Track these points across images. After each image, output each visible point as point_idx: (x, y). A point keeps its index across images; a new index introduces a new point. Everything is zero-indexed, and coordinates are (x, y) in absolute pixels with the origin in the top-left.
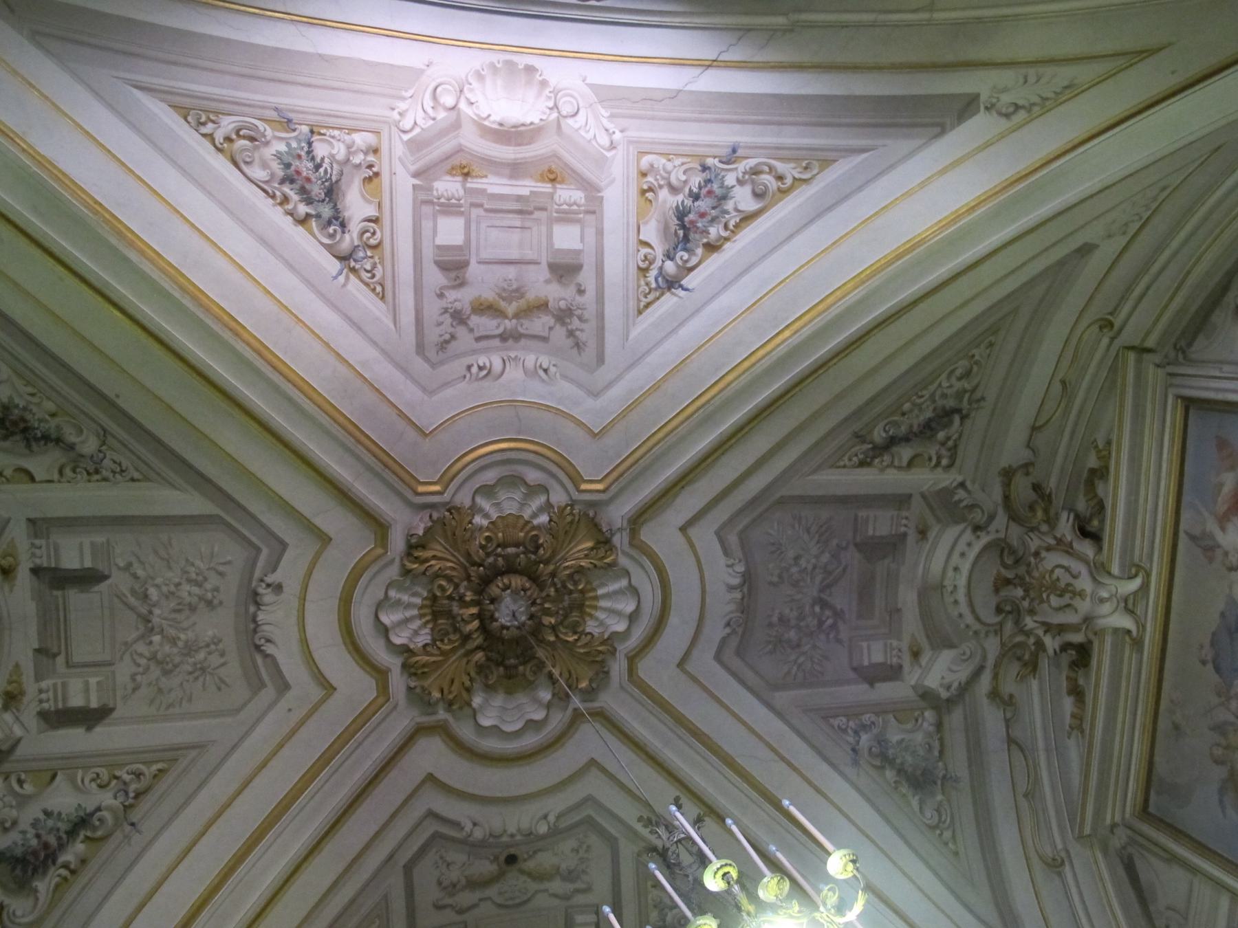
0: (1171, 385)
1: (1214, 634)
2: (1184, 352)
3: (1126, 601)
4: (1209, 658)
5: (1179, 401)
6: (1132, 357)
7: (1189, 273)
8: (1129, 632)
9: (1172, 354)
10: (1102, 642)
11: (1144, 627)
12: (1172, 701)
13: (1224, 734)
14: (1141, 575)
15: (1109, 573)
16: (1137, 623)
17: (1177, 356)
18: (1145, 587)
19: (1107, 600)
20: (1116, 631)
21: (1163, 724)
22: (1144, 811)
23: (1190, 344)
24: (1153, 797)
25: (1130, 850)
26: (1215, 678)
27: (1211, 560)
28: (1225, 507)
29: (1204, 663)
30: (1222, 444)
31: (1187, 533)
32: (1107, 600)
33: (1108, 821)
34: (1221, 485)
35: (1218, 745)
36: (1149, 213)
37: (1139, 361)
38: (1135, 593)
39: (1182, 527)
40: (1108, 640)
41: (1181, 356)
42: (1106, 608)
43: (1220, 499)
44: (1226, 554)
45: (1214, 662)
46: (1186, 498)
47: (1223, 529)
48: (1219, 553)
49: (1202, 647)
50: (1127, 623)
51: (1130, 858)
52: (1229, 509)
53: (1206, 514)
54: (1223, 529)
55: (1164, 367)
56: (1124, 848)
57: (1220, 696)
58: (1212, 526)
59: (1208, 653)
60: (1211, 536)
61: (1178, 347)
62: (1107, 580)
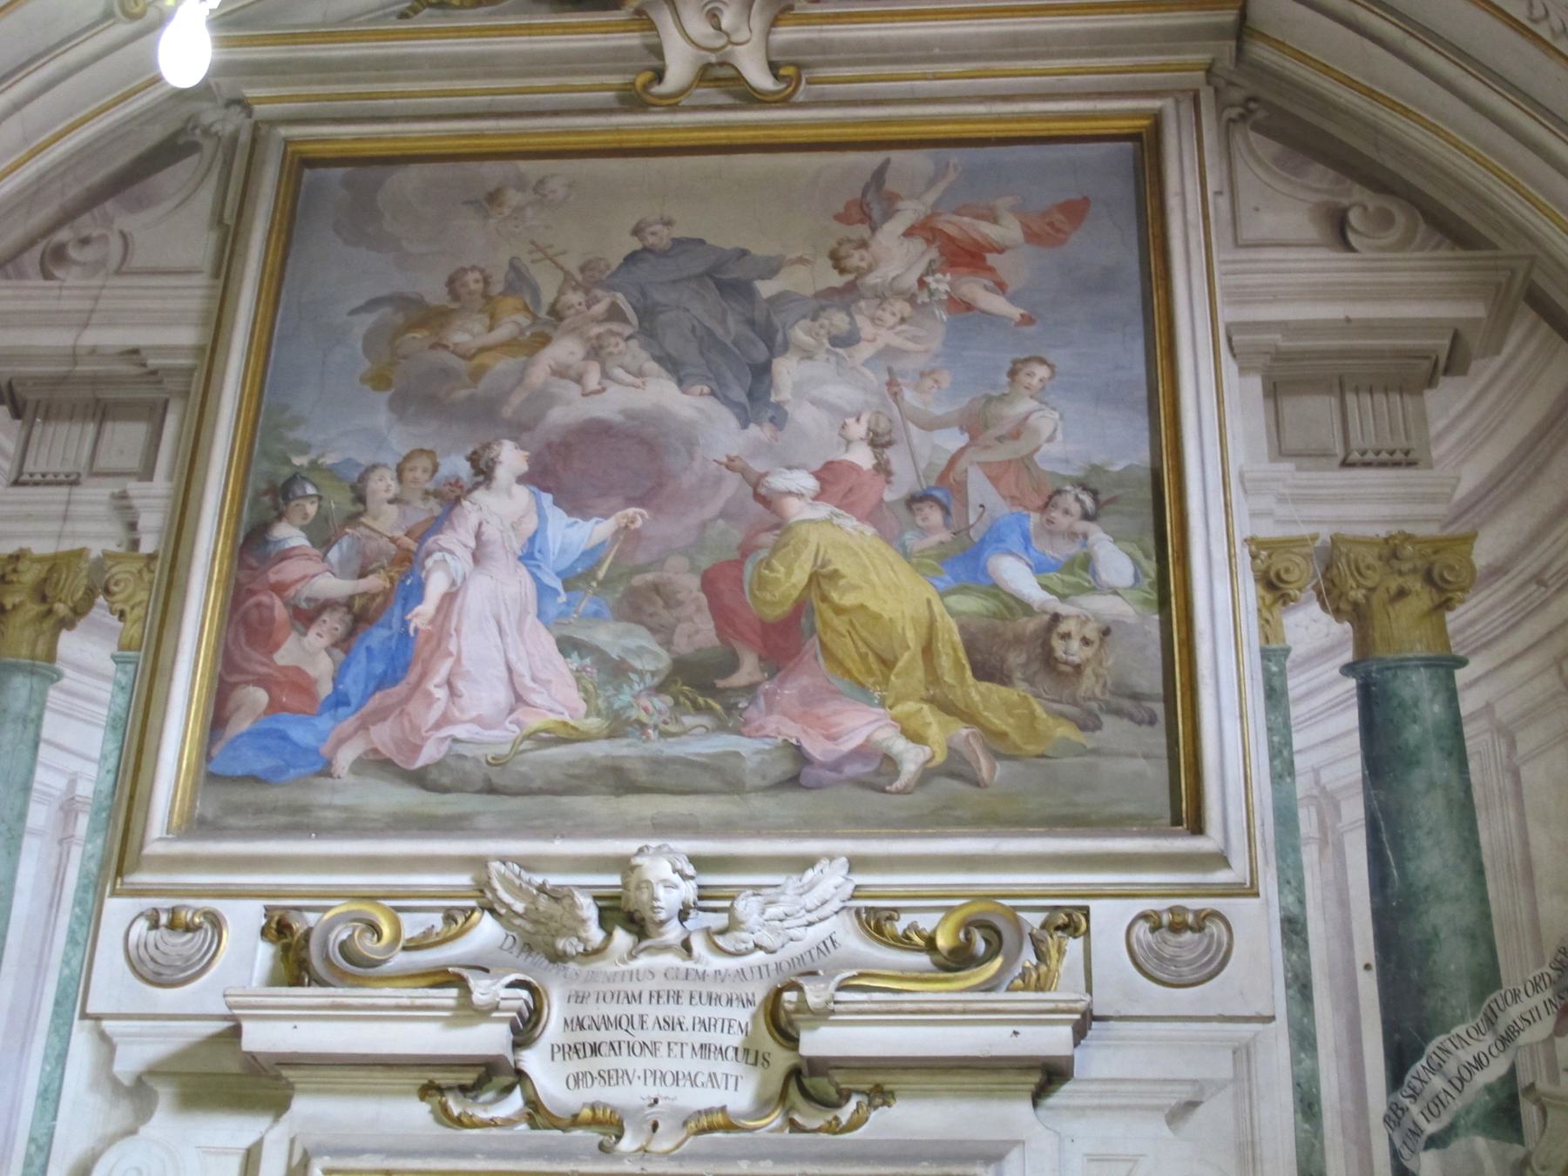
0: (1177, 102)
1: (701, 242)
2: (1243, 117)
3: (722, 64)
4: (651, 240)
5: (1145, 122)
6: (1228, 17)
7: (1406, 112)
8: (659, 75)
9: (1236, 95)
10: (623, 27)
11: (674, 108)
12: (541, 182)
13: (510, 289)
14: (782, 86)
15: (774, 23)
16: (683, 92)
17: (1232, 105)
18: (751, 98)
19: (718, 28)
20: (657, 51)
21: (493, 172)
22: (301, 163)
23: (1257, 128)
24: (338, 172)
25: (208, 145)
26: (616, 260)
27: (841, 218)
28: (951, 230)
29: (637, 231)
30: (1075, 211)
31: (887, 162)
32: (718, 28)
33: (250, 93)
34: (995, 220)
35: (486, 281)
36: (1547, 36)
37: (1217, 32)
38: (739, 78)
39: (896, 156)
40: (633, 40)
41: (1234, 112)
42: (698, 27)
43: (966, 219)
44: (863, 244)
45: (645, 249)
46: (955, 156)
47: (909, 233)
48: (862, 231)
49: (668, 223)
50: (678, 70)
51: (193, 147)
52: (950, 239)
53: (931, 197)
54: (909, 233)
55: (1209, 83)
56: (206, 132)
57: (582, 269)
58: (910, 212)
59: (660, 237)
60: (888, 215)
61: (1252, 105)
62: (758, 22)
